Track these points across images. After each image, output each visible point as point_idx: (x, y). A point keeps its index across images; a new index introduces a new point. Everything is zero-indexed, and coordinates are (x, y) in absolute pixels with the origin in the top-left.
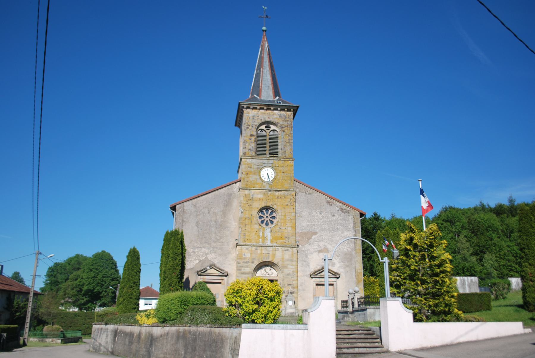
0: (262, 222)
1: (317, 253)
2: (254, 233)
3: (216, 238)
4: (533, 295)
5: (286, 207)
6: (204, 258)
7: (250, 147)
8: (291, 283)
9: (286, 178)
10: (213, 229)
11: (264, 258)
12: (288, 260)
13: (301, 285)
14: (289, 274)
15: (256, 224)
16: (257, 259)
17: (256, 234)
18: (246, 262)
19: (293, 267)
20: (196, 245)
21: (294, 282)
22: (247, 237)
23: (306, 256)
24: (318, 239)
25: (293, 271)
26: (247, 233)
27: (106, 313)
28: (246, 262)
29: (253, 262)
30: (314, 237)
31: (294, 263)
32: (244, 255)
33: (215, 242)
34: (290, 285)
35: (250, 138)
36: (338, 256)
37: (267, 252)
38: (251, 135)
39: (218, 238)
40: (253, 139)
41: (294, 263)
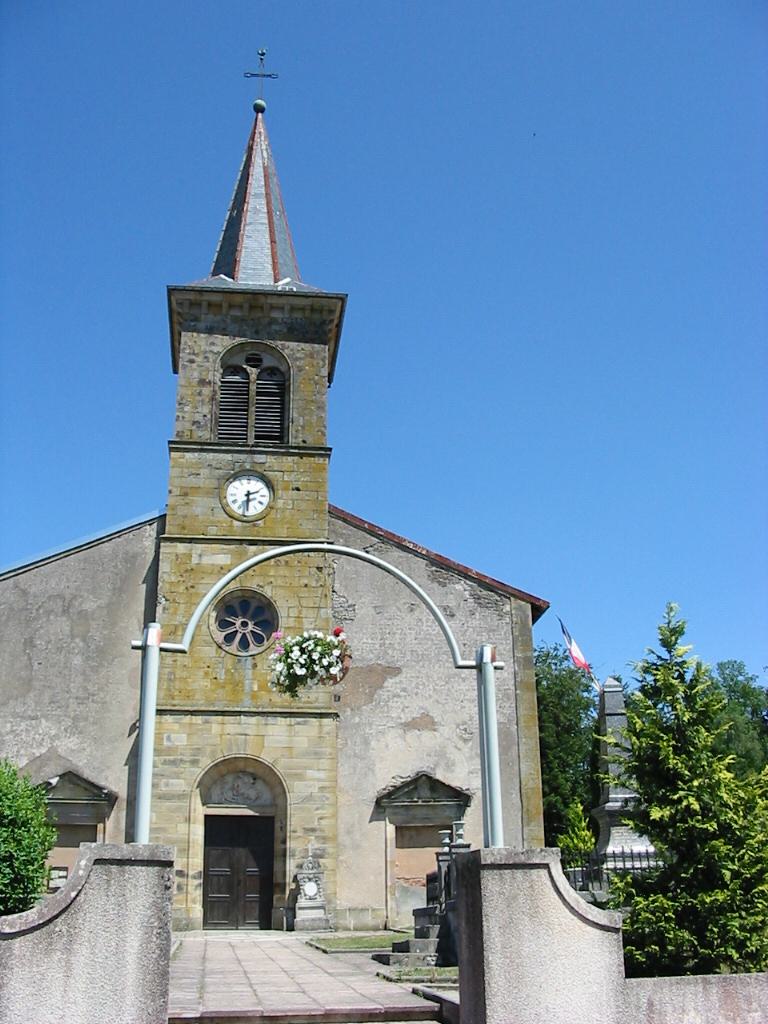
0: (229, 638)
1: (401, 731)
2: (201, 673)
3: (85, 689)
4: (766, 778)
5: (304, 593)
6: (43, 750)
7: (198, 417)
8: (315, 824)
9: (303, 506)
10: (77, 661)
11: (230, 749)
12: (306, 754)
13: (349, 832)
14: (310, 798)
15: (207, 644)
16: (208, 750)
17: (206, 674)
18: (173, 763)
19: (322, 775)
20: (20, 710)
21: (323, 822)
22: (177, 684)
23: (366, 742)
24: (404, 690)
25: (322, 789)
26: (179, 673)
27: (159, 798)
28: (173, 763)
29: (194, 762)
30: (390, 683)
31: (325, 763)
32: (169, 738)
33: (81, 701)
34: (313, 830)
35: (198, 389)
36: (465, 741)
37: (239, 729)
38: (203, 382)
39: (91, 688)
40: (207, 391)
41: (325, 763)
